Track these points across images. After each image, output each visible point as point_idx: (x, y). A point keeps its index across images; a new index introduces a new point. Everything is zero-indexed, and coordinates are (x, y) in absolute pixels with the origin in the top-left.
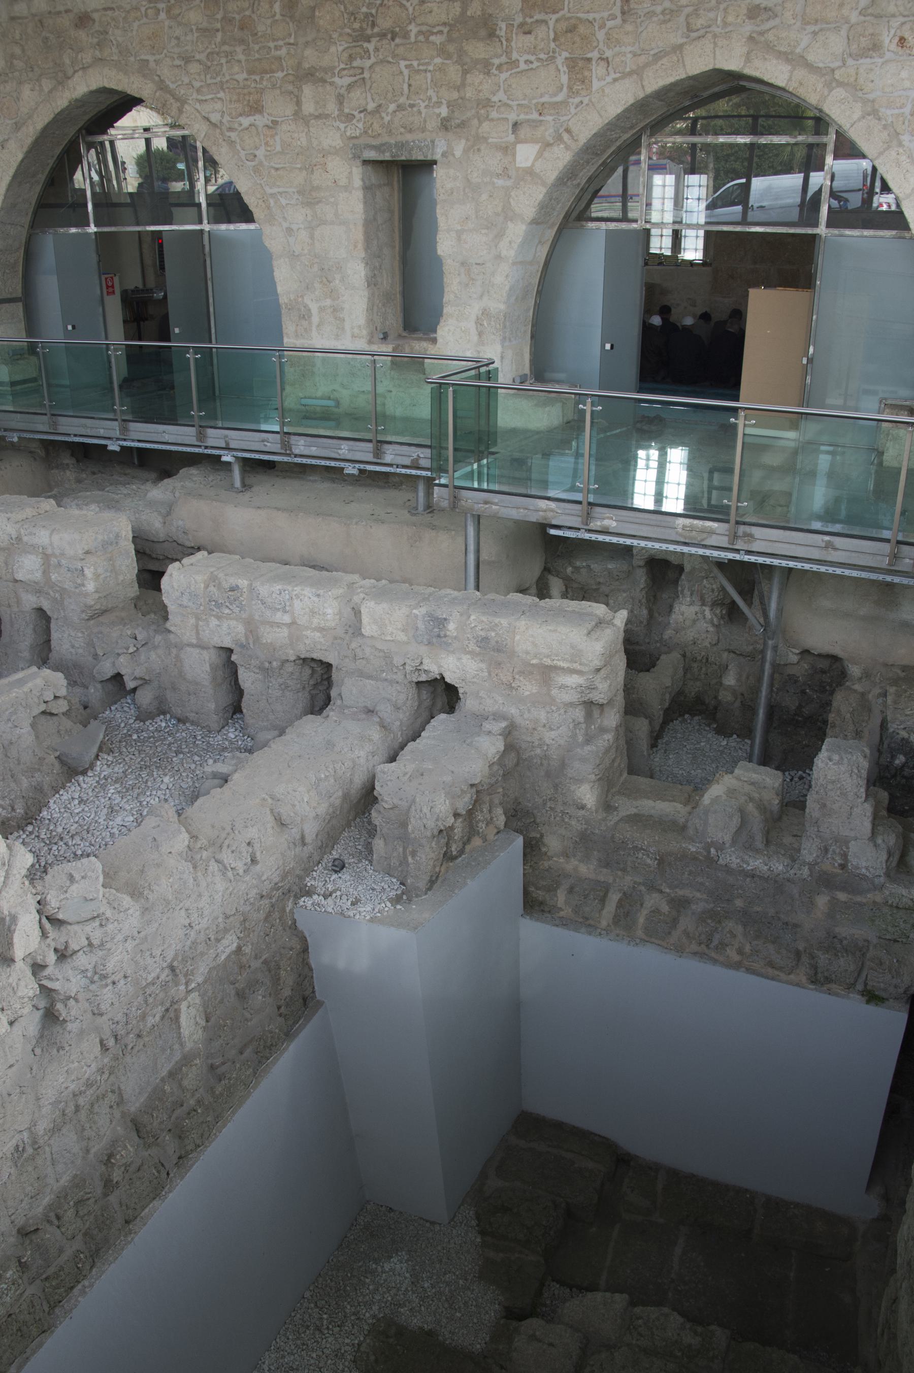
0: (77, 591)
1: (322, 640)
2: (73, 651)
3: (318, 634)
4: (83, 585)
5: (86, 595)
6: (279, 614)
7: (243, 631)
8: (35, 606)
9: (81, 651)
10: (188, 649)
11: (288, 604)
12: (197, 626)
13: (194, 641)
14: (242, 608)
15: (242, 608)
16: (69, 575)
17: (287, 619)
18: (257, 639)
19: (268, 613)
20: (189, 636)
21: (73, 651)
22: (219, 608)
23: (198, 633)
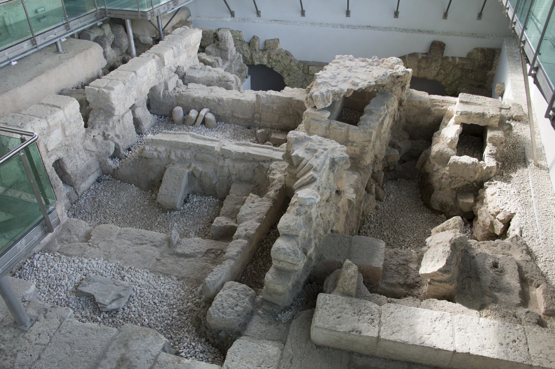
13: (124, 112)
17: (146, 77)
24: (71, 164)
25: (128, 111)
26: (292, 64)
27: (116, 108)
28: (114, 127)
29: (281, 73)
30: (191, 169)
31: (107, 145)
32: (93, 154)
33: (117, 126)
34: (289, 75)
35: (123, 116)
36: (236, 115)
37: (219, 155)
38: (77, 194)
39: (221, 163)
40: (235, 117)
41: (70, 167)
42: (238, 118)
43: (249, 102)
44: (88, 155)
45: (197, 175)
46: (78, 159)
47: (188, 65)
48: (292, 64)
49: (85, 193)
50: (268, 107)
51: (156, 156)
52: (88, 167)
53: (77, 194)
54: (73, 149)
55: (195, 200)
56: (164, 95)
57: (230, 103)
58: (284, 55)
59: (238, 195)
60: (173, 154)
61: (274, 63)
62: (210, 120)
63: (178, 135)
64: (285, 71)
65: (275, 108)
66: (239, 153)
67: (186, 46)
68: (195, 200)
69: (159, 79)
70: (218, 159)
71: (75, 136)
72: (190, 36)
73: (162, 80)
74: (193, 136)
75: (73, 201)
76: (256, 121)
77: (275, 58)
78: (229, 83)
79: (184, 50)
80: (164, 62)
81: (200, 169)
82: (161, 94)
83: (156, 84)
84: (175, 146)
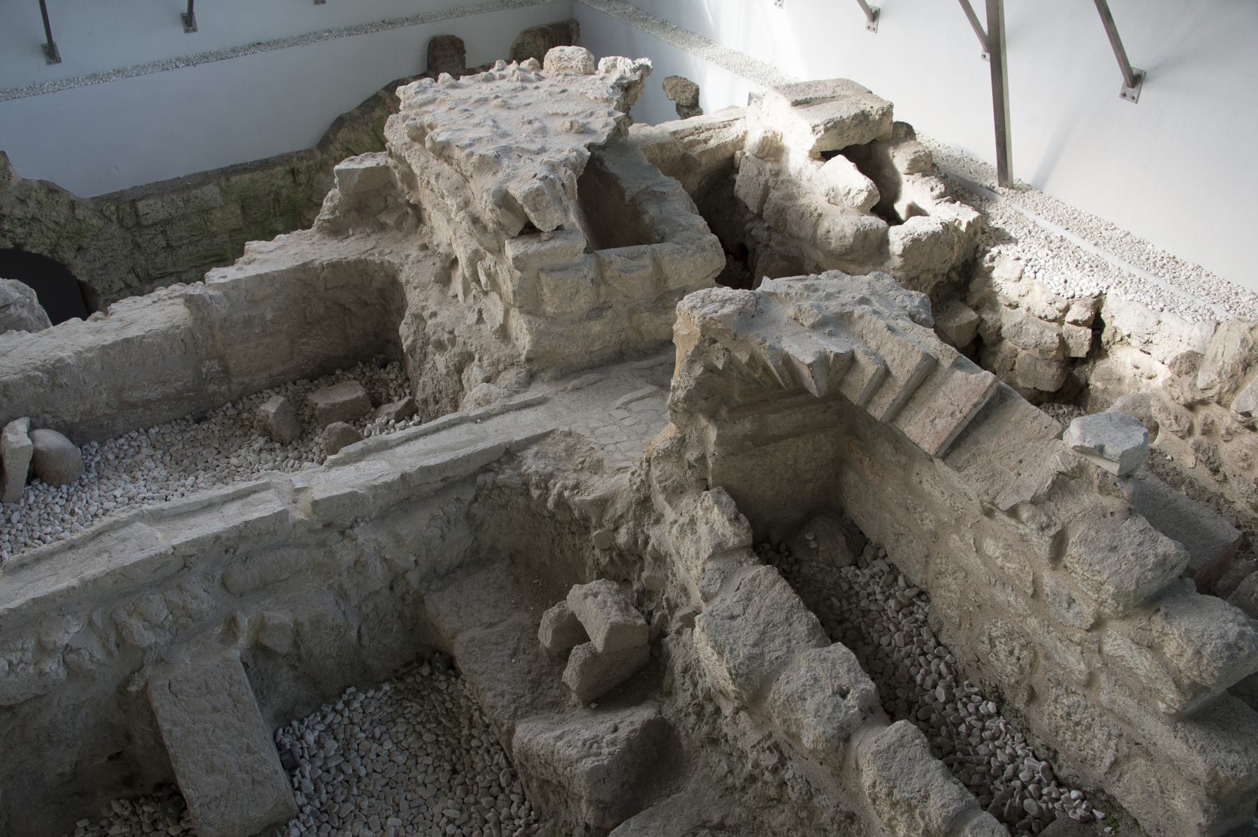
26: (80, 213)
29: (52, 251)
30: (243, 641)
34: (80, 249)
36: (134, 396)
37: (311, 531)
39: (346, 555)
40: (134, 406)
42: (147, 403)
43: (165, 335)
45: (282, 644)
48: (80, 213)
50: (248, 322)
51: (62, 673)
55: (311, 737)
57: (97, 366)
58: (42, 195)
59: (490, 625)
60: (136, 624)
61: (19, 230)
62: (61, 453)
63: (92, 547)
64: (65, 243)
65: (269, 316)
66: (388, 486)
68: (311, 737)
70: (322, 544)
74: (157, 518)
76: (212, 388)
77: (18, 212)
78: (12, 310)
81: (280, 617)
84: (123, 589)
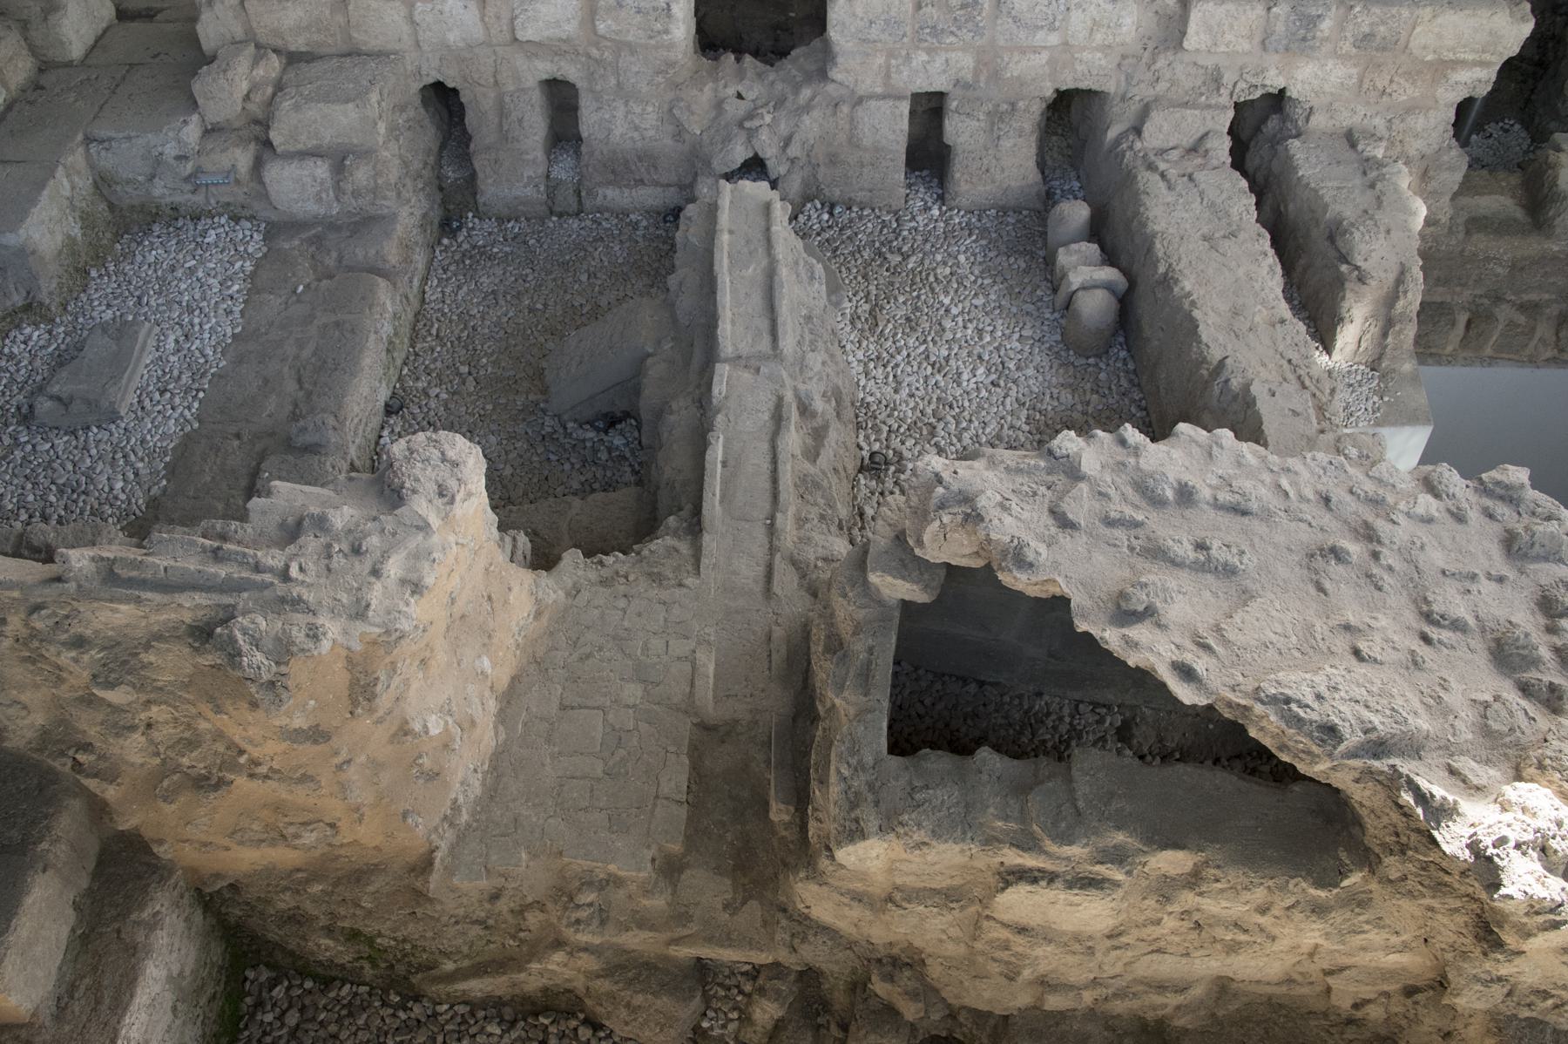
0: (653, 42)
1: (1103, 62)
2: (636, 135)
3: (1099, 55)
4: (667, 32)
5: (671, 46)
6: (1040, 35)
7: (972, 65)
8: (545, 77)
9: (651, 133)
10: (873, 103)
11: (1060, 17)
12: (888, 67)
13: (879, 90)
14: (978, 31)
15: (978, 31)
16: (639, 18)
17: (1054, 39)
18: (996, 75)
19: (1022, 35)
20: (870, 83)
21: (636, 135)
22: (936, 36)
23: (888, 76)
24: (595, 117)
25: (899, 98)
27: (840, 60)
28: (807, 108)
31: (727, 139)
32: (687, 137)
33: (816, 113)
35: (860, 101)
38: (580, 202)
41: (590, 119)
44: (670, 128)
46: (620, 113)
47: (1346, 120)
49: (607, 215)
52: (648, 158)
53: (580, 202)
54: (613, 81)
56: (1118, 141)
67: (1368, 37)
69: (1129, 78)
71: (632, 49)
72: (1427, 12)
73: (1143, 92)
75: (557, 209)
79: (1347, 47)
80: (1184, 33)
82: (1112, 134)
83: (1110, 86)
